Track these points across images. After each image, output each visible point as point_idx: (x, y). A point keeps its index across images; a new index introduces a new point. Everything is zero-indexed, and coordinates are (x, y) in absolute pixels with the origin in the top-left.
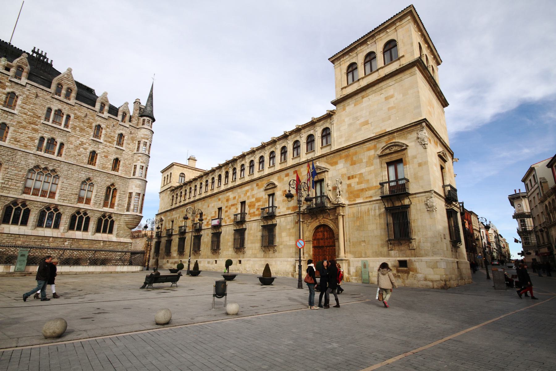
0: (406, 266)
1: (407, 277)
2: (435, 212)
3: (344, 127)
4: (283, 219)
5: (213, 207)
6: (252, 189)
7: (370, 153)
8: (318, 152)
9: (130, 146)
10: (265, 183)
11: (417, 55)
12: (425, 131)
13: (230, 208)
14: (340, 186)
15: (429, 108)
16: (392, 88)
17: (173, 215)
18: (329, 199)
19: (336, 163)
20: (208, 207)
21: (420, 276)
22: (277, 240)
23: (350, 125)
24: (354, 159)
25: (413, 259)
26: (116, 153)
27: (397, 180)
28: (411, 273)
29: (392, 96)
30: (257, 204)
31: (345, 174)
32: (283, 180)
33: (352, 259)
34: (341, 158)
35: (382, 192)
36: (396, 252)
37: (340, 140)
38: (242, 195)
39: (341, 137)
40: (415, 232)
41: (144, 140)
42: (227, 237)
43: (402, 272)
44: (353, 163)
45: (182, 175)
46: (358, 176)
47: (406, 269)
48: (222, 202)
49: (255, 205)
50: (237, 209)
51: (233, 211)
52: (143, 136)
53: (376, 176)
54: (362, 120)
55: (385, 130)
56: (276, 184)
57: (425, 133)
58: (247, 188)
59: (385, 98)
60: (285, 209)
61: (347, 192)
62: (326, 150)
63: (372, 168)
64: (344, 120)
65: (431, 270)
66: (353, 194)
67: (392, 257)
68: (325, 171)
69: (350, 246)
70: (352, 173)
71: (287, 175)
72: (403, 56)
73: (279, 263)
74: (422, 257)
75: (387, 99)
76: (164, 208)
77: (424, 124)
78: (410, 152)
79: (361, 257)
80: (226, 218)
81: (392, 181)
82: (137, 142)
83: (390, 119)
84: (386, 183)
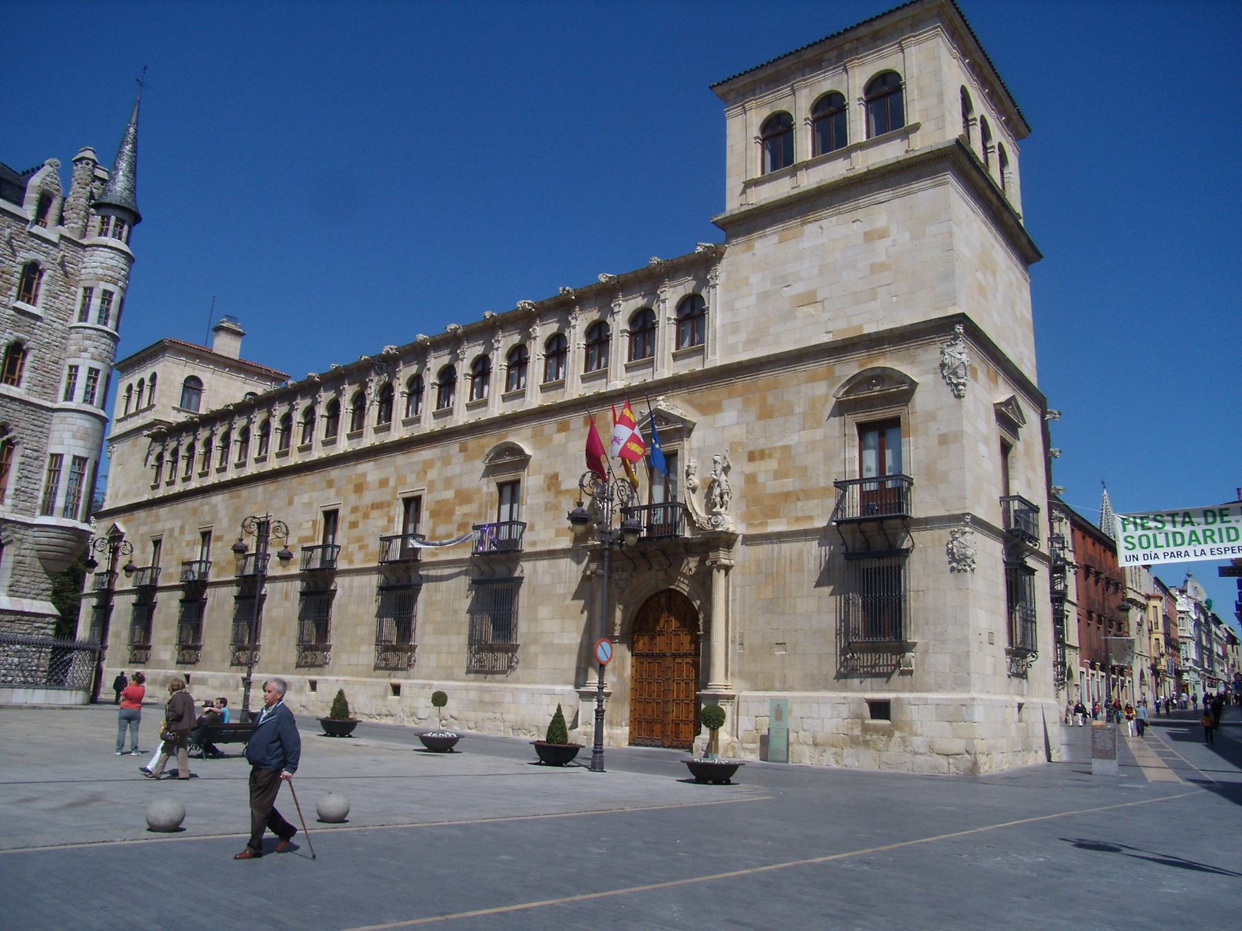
0: (887, 717)
1: (887, 745)
2: (969, 574)
3: (747, 303)
4: (542, 564)
5: (308, 505)
6: (446, 461)
7: (818, 389)
8: (666, 368)
9: (58, 304)
10: (490, 442)
11: (954, 130)
12: (960, 346)
13: (366, 516)
14: (723, 478)
15: (979, 275)
16: (884, 211)
17: (158, 519)
18: (689, 515)
19: (716, 408)
20: (291, 503)
21: (918, 742)
22: (523, 626)
23: (764, 296)
24: (770, 400)
25: (905, 695)
26: (16, 325)
27: (881, 477)
28: (897, 734)
29: (883, 234)
30: (460, 511)
31: (741, 444)
32: (550, 440)
33: (745, 693)
34: (730, 396)
35: (840, 506)
37: (731, 340)
38: (411, 478)
40: (917, 625)
41: (103, 286)
42: (352, 608)
43: (876, 730)
44: (766, 414)
45: (193, 386)
47: (886, 722)
48: (338, 493)
49: (450, 513)
50: (391, 520)
51: (376, 525)
52: (100, 271)
53: (828, 458)
54: (799, 288)
55: (861, 327)
56: (528, 451)
57: (961, 353)
58: (427, 454)
59: (866, 234)
60: (552, 533)
61: (742, 497)
62: (692, 365)
63: (818, 434)
64: (747, 278)
65: (947, 724)
66: (760, 504)
68: (685, 429)
69: (741, 655)
70: (762, 443)
71: (563, 428)
72: (916, 127)
73: (524, 698)
74: (929, 691)
75: (869, 237)
76: (126, 495)
77: (959, 329)
78: (920, 400)
79: (772, 689)
80: (353, 548)
81: (870, 480)
82: (81, 292)
83: (875, 299)
84: (853, 482)
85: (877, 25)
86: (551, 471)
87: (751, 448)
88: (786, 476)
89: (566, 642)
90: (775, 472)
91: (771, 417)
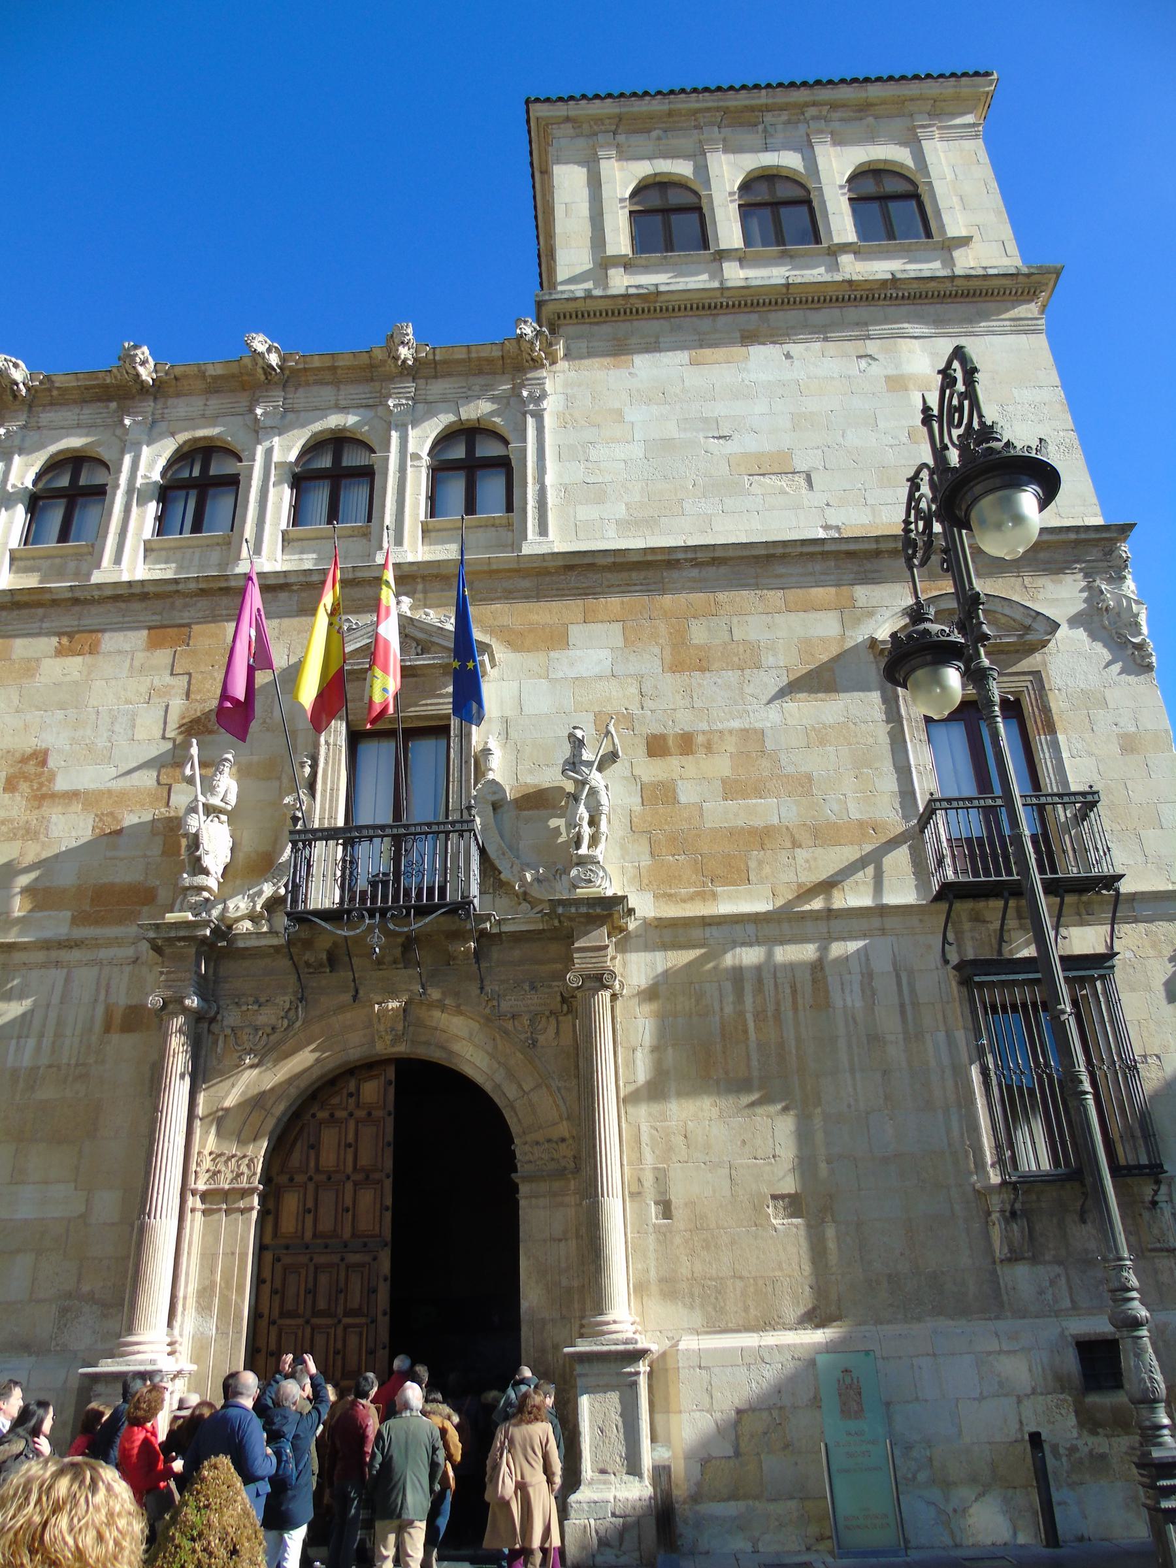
19: (557, 639)
33: (689, 1343)
36: (1044, 1272)
39: (597, 493)
46: (730, 745)
67: (1021, 1314)
85: (874, 92)
86: (29, 744)
87: (657, 729)
88: (759, 790)
89: (26, 1212)
90: (724, 781)
91: (702, 670)
